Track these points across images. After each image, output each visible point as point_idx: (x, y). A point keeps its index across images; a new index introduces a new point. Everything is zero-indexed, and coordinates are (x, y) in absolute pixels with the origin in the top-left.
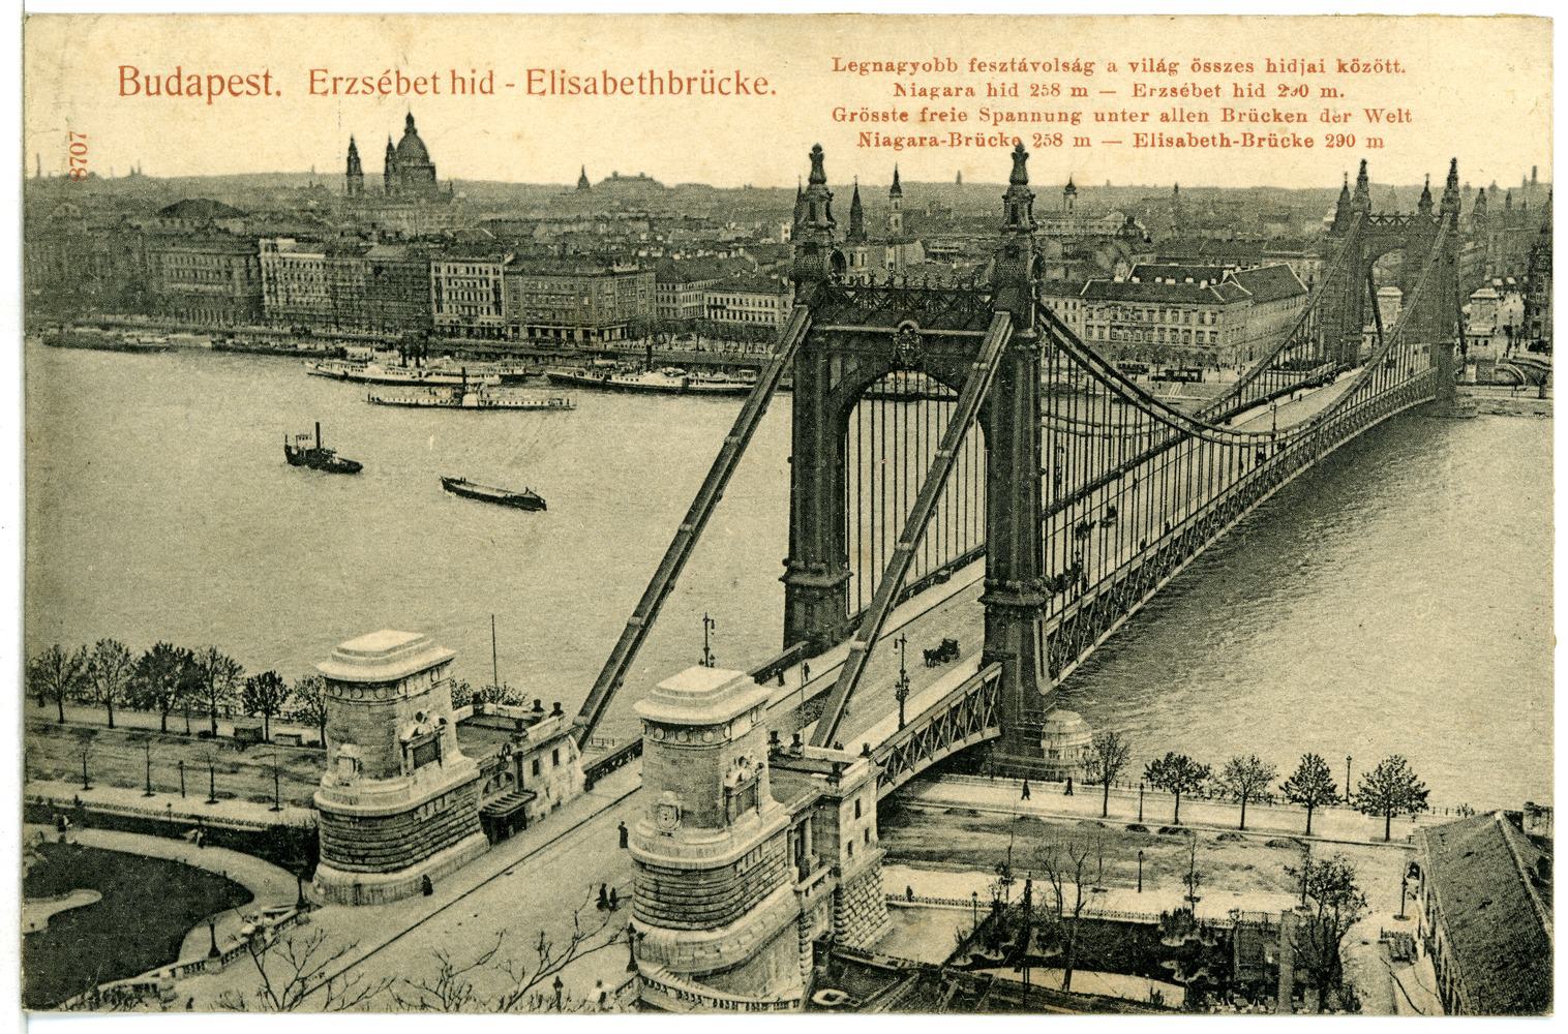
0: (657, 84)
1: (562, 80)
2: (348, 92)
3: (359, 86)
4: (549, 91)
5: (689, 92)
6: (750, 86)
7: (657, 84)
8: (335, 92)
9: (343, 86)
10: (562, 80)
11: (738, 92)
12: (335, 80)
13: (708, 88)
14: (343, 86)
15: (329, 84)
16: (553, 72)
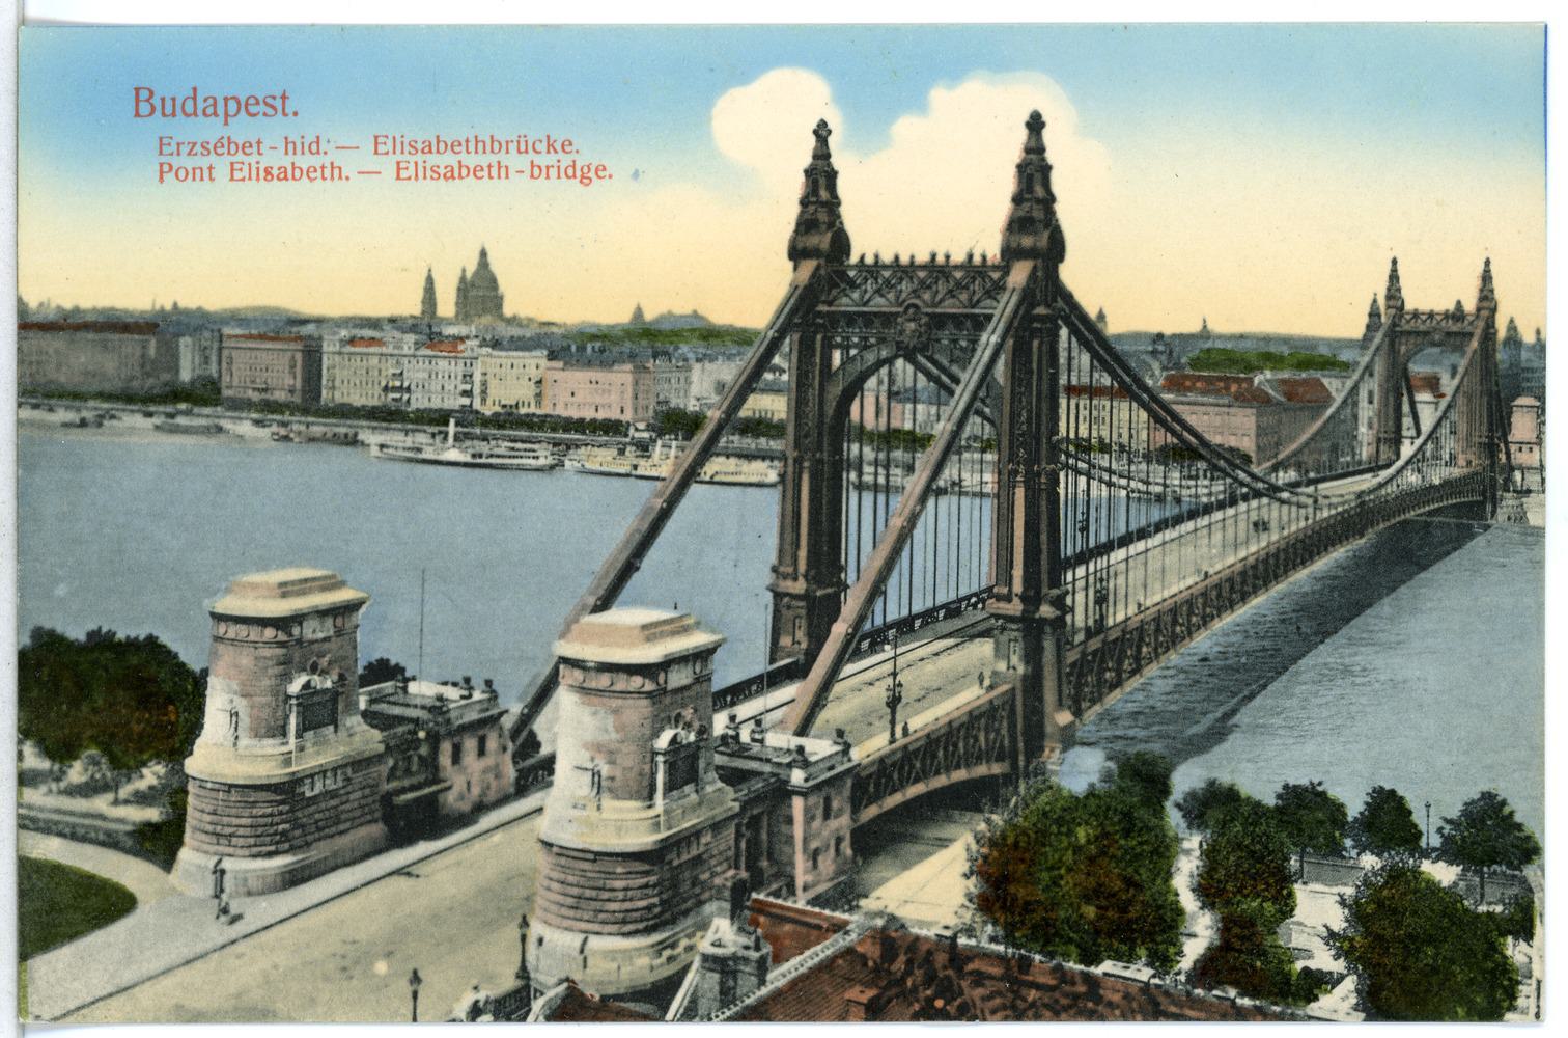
0: (480, 146)
1: (402, 144)
2: (189, 154)
3: (198, 148)
4: (391, 150)
5: (507, 152)
6: (558, 146)
7: (480, 146)
8: (179, 154)
9: (185, 149)
10: (402, 144)
11: (548, 152)
12: (178, 144)
13: (523, 148)
14: (185, 149)
15: (174, 148)
16: (394, 138)
